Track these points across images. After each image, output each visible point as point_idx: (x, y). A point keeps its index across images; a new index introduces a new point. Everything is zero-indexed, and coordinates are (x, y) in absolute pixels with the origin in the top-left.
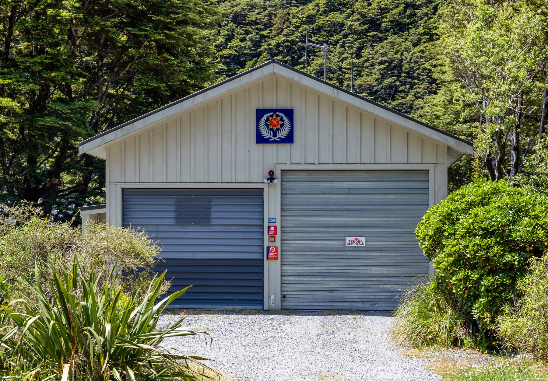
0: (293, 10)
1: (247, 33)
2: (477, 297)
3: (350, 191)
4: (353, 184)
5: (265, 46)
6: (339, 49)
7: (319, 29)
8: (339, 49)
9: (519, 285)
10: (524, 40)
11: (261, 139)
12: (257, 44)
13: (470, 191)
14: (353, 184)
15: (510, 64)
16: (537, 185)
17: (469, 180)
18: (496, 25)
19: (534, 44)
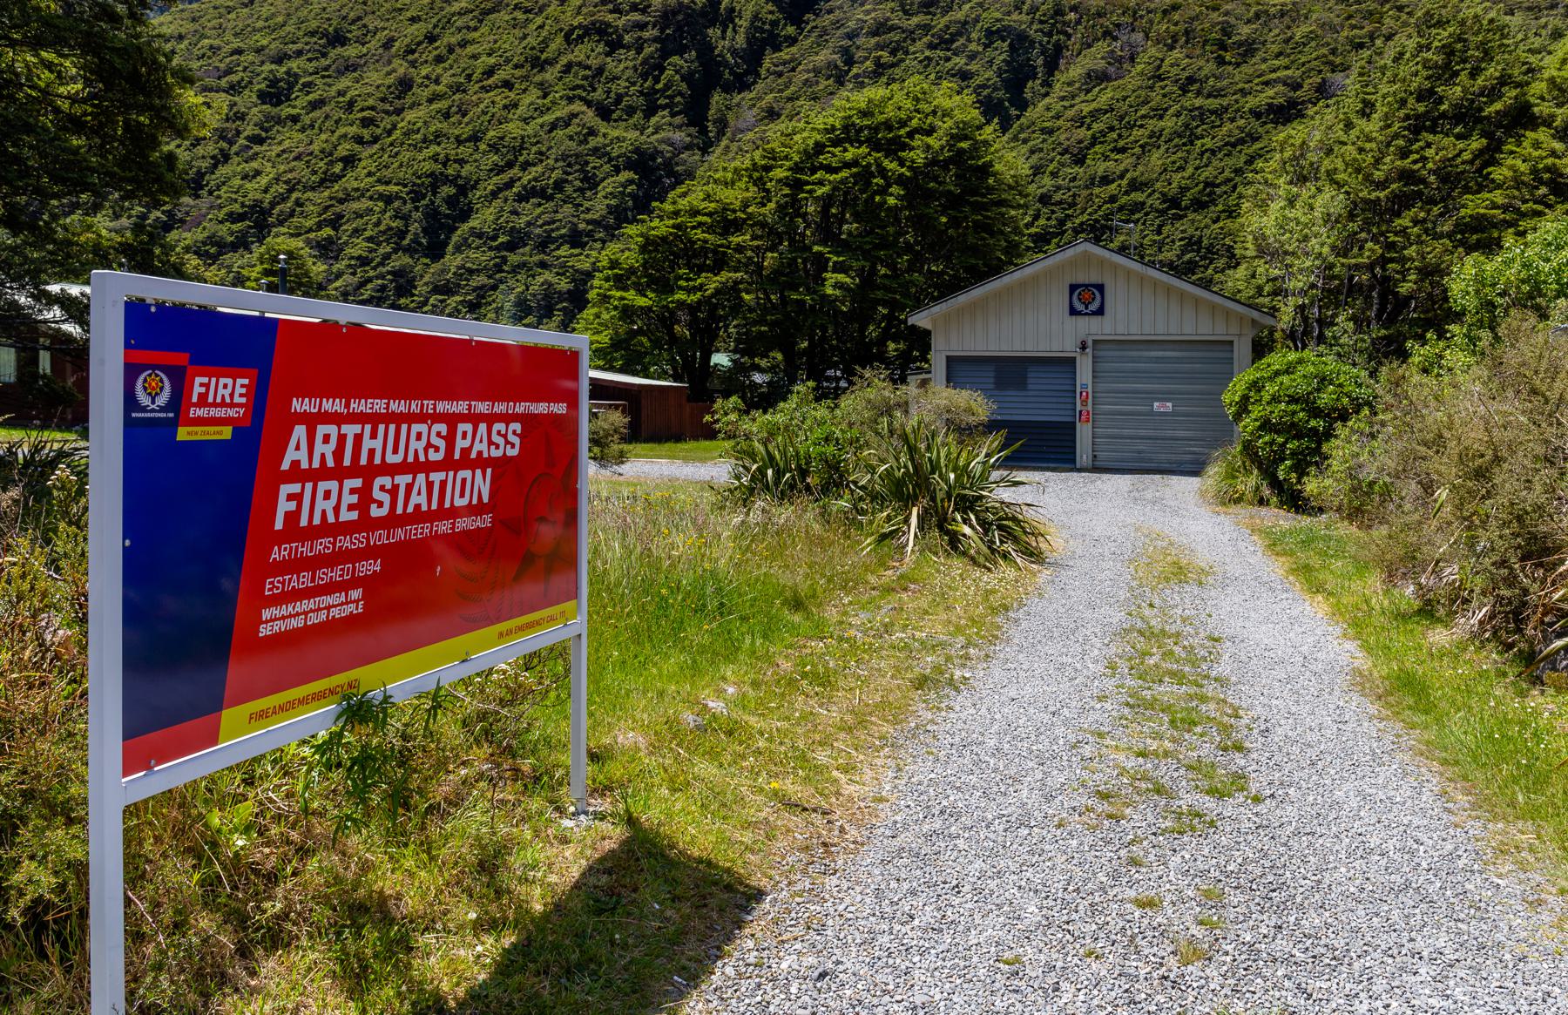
0: (1097, 190)
1: (1053, 212)
2: (1283, 460)
3: (1158, 360)
4: (1160, 354)
5: (1069, 225)
6: (1140, 227)
7: (1121, 208)
8: (1140, 227)
9: (1325, 448)
10: (1327, 218)
11: (1073, 312)
12: (1062, 223)
13: (1276, 360)
14: (1160, 354)
15: (1314, 241)
16: (1339, 355)
17: (1271, 350)
18: (1298, 204)
19: (1337, 221)
